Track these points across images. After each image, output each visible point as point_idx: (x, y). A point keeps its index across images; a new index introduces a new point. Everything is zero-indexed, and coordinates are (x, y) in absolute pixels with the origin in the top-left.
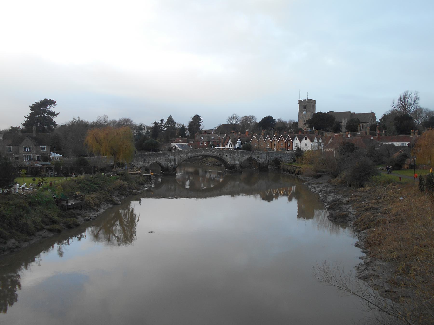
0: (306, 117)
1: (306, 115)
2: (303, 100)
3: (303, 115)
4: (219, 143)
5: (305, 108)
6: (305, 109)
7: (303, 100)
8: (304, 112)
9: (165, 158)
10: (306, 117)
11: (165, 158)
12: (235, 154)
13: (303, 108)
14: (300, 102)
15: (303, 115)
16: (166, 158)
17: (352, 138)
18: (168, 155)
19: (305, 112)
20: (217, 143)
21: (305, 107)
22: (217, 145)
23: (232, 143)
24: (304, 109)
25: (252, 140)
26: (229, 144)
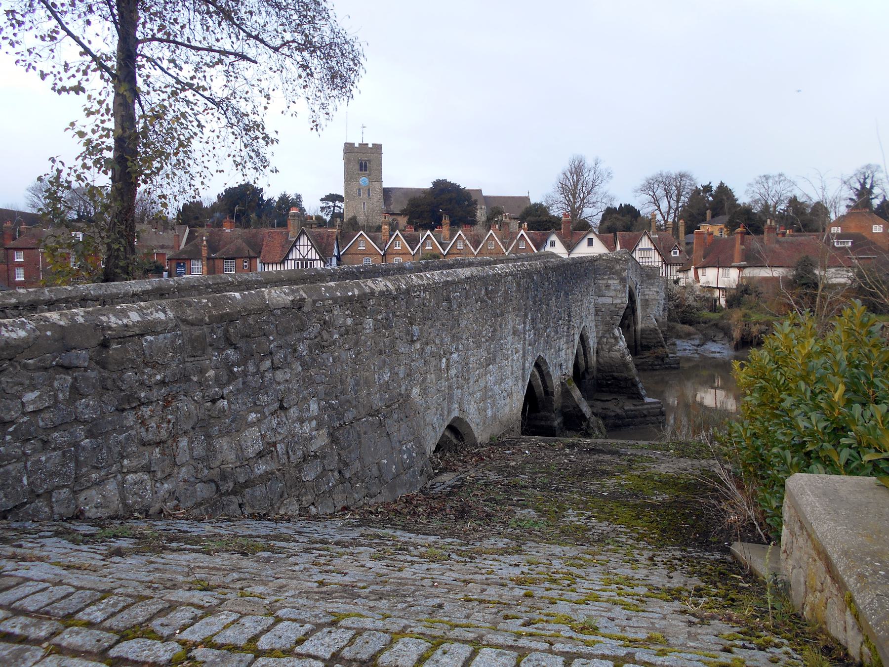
0: (369, 195)
1: (369, 189)
2: (360, 144)
3: (359, 190)
4: (184, 256)
5: (363, 167)
6: (366, 170)
7: (357, 145)
8: (364, 181)
9: (601, 300)
10: (369, 195)
11: (601, 300)
12: (652, 284)
13: (358, 167)
14: (349, 148)
15: (359, 190)
16: (609, 301)
17: (794, 239)
18: (624, 274)
19: (367, 181)
20: (177, 259)
21: (366, 166)
22: (178, 265)
23: (313, 255)
24: (361, 170)
25: (350, 249)
26: (291, 260)
